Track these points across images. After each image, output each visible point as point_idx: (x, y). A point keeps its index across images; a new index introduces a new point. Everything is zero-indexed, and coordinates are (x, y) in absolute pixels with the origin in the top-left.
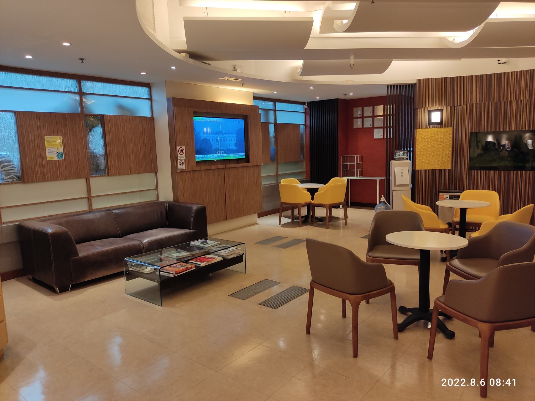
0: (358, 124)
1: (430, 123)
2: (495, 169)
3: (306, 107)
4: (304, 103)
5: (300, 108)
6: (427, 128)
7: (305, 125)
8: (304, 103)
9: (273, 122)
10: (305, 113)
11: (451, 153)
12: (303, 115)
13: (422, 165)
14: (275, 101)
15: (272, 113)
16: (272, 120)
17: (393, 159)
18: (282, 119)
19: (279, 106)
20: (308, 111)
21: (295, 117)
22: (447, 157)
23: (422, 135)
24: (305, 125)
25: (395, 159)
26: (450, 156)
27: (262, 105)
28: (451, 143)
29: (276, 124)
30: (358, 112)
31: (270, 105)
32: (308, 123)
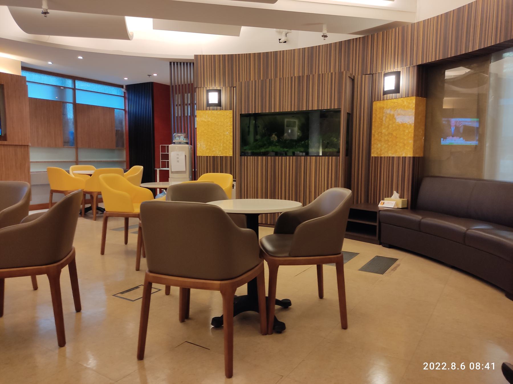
0: (177, 111)
1: (209, 105)
2: (265, 154)
3: (123, 90)
4: (122, 87)
5: (120, 92)
6: (207, 110)
7: (125, 110)
8: (122, 87)
9: (72, 101)
10: (125, 97)
11: (232, 138)
12: (123, 99)
13: (203, 150)
14: (74, 78)
15: (70, 93)
16: (70, 99)
17: (171, 142)
18: (82, 99)
19: (79, 85)
20: (127, 96)
21: (115, 101)
22: (228, 143)
23: (202, 118)
24: (125, 110)
25: (174, 143)
26: (232, 141)
27: (30, 76)
28: (232, 127)
29: (75, 105)
30: (177, 99)
31: (69, 83)
32: (127, 109)
